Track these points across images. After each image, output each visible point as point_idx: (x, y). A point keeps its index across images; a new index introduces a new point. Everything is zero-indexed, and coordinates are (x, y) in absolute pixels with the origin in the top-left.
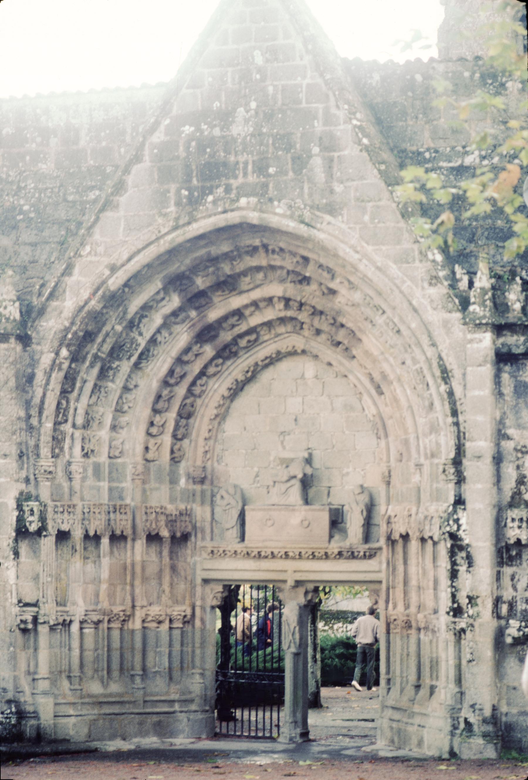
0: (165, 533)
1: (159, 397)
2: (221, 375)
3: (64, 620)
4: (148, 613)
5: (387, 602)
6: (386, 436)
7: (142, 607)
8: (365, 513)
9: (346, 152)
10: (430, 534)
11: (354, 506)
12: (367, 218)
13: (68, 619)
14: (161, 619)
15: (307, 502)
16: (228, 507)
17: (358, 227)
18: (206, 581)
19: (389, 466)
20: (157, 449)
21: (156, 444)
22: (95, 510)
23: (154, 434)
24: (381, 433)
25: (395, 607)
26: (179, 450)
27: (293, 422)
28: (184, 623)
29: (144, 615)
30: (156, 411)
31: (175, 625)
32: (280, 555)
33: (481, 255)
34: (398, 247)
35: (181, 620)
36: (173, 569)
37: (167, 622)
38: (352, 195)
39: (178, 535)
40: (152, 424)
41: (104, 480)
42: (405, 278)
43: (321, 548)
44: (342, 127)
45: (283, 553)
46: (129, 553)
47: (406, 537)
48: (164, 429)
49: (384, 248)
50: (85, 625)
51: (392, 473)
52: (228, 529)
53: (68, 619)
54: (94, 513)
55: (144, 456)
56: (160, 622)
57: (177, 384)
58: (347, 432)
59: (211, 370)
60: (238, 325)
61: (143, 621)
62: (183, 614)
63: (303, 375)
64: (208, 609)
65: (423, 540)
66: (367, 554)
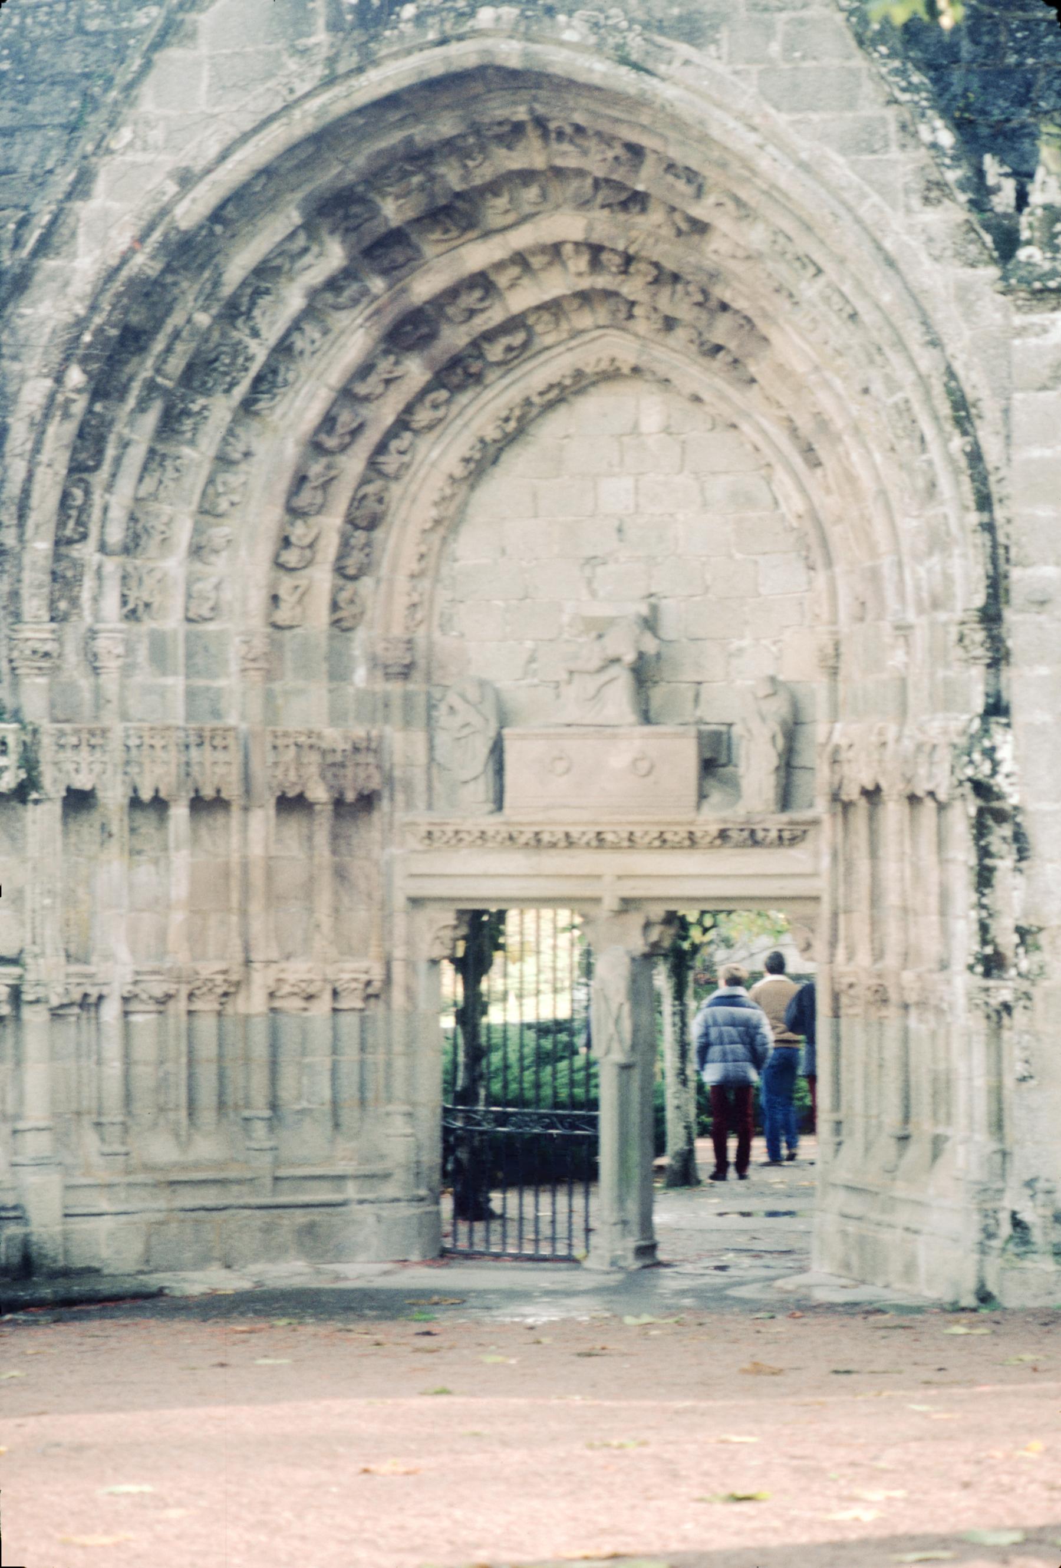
0: (319, 793)
1: (301, 480)
2: (446, 429)
3: (86, 996)
4: (282, 976)
5: (833, 944)
6: (829, 563)
7: (269, 962)
8: (780, 742)
10: (930, 787)
11: (755, 725)
12: (775, 48)
13: (94, 992)
14: (312, 990)
15: (646, 717)
17: (755, 69)
18: (416, 902)
19: (835, 633)
20: (300, 601)
21: (296, 587)
22: (153, 742)
23: (292, 565)
24: (817, 555)
25: (850, 957)
26: (352, 601)
28: (368, 997)
29: (271, 983)
30: (294, 512)
31: (343, 1004)
32: (585, 839)
33: (1044, 129)
34: (849, 115)
36: (340, 874)
37: (327, 996)
39: (350, 796)
40: (286, 542)
42: (867, 189)
43: (678, 824)
45: (591, 835)
46: (235, 840)
47: (873, 795)
48: (314, 553)
49: (815, 117)
50: (134, 1006)
51: (843, 649)
52: (466, 782)
53: (94, 992)
54: (152, 747)
55: (269, 615)
56: (310, 997)
57: (343, 448)
58: (738, 556)
59: (423, 416)
60: (482, 310)
61: (272, 995)
62: (364, 978)
63: (636, 425)
64: (423, 966)
65: (913, 799)
66: (786, 835)
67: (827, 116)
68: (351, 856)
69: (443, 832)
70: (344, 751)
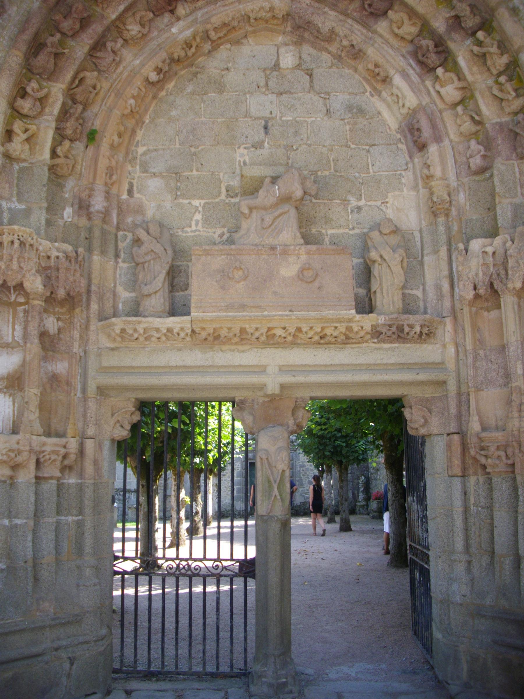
14: (19, 459)
15: (308, 239)
16: (148, 258)
23: (25, 111)
27: (262, 131)
31: (46, 472)
32: (257, 334)
35: (58, 463)
39: (61, 293)
43: (339, 321)
48: (43, 108)
52: (149, 295)
62: (63, 451)
63: (276, 67)
68: (54, 351)
69: (135, 330)
70: (58, 257)
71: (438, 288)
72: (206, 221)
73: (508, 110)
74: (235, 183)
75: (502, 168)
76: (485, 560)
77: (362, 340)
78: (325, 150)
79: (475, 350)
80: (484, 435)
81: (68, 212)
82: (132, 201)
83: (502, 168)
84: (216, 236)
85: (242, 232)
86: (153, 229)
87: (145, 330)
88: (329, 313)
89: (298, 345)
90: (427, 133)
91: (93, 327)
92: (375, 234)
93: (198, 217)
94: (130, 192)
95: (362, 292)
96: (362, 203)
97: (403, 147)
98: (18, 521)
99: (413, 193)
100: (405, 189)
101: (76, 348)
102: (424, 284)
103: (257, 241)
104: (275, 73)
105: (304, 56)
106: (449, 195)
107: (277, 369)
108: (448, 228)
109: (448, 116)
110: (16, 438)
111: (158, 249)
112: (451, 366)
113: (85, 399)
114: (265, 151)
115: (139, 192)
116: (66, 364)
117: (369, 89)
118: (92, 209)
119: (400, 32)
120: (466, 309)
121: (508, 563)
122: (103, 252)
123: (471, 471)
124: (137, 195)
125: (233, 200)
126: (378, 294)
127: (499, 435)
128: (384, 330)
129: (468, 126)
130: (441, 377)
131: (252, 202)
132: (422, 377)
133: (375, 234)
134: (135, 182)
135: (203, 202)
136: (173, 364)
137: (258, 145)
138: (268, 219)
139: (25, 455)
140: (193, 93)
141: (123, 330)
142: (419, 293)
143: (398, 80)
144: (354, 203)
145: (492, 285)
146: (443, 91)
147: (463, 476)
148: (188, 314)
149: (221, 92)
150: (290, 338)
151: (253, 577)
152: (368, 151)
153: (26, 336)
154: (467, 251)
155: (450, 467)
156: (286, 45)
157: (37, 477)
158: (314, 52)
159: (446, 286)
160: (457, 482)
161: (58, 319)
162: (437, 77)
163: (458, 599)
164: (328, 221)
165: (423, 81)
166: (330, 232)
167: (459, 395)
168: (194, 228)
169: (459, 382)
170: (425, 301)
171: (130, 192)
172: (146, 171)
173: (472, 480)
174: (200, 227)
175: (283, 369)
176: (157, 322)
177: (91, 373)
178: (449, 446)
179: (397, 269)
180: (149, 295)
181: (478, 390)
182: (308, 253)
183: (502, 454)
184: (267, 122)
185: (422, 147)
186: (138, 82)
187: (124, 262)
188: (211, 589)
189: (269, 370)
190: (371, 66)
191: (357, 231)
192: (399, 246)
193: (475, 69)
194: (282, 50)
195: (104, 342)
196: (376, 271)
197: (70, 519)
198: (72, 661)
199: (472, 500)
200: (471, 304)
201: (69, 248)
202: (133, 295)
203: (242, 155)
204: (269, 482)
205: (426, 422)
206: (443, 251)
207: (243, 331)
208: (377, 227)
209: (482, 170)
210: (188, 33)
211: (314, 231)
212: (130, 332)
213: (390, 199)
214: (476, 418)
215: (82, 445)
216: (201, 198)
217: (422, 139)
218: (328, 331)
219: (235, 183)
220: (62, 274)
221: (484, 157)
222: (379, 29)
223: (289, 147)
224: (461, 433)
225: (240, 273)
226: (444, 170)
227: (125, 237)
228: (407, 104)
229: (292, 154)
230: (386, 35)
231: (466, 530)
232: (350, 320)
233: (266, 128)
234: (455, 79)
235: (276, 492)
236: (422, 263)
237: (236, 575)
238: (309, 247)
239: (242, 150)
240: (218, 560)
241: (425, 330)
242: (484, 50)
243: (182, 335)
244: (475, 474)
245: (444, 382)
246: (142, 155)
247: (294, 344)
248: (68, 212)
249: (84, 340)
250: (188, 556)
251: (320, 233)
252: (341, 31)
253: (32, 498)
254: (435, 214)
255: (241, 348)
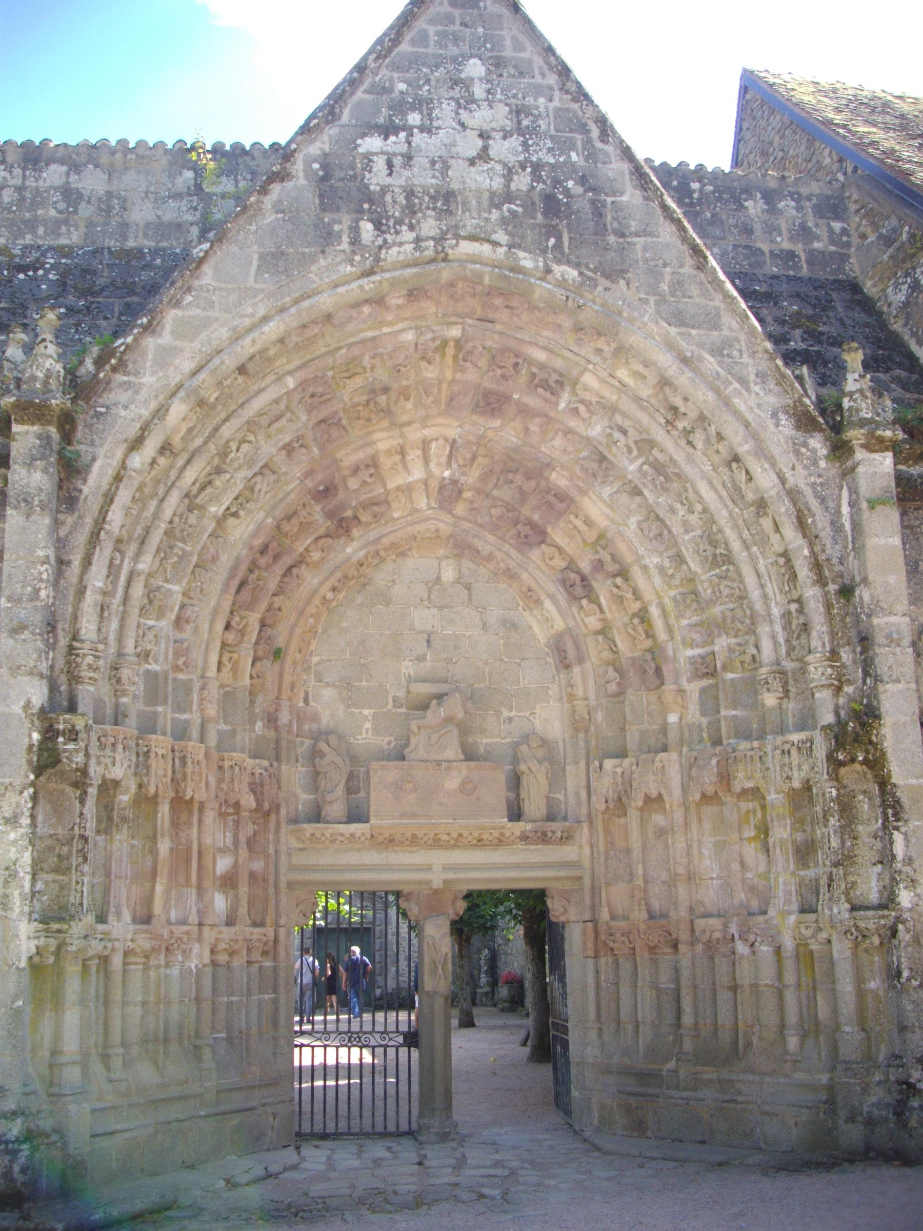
4: (221, 936)
7: (212, 926)
9: (624, 198)
12: (664, 287)
14: (236, 947)
17: (652, 299)
18: (291, 885)
19: (588, 706)
23: (229, 642)
27: (425, 645)
29: (212, 941)
32: (425, 839)
34: (715, 333)
37: (245, 952)
38: (639, 255)
40: (228, 627)
41: (165, 703)
42: (730, 378)
43: (494, 828)
44: (614, 166)
45: (431, 836)
48: (243, 636)
49: (693, 332)
50: (132, 959)
52: (331, 802)
57: (268, 567)
61: (212, 952)
62: (265, 939)
63: (438, 579)
67: (702, 332)
69: (323, 835)
71: (577, 795)
72: (376, 730)
73: (639, 647)
74: (401, 694)
75: (633, 698)
76: (613, 1027)
77: (513, 843)
78: (481, 664)
79: (607, 852)
80: (612, 923)
81: (259, 725)
82: (308, 708)
83: (633, 698)
84: (384, 744)
85: (411, 747)
86: (332, 739)
87: (332, 835)
88: (485, 821)
89: (458, 847)
90: (571, 654)
91: (283, 830)
92: (524, 748)
93: (368, 725)
94: (306, 700)
95: (512, 795)
96: (514, 713)
97: (550, 660)
98: (234, 999)
99: (558, 705)
100: (551, 702)
101: (271, 850)
102: (565, 789)
103: (425, 757)
104: (437, 587)
105: (465, 571)
106: (589, 714)
107: (440, 867)
108: (587, 742)
109: (590, 640)
110: (233, 929)
111: (338, 760)
112: (587, 864)
113: (277, 893)
114: (428, 665)
115: (314, 701)
116: (262, 864)
117: (521, 603)
118: (279, 723)
119: (552, 563)
120: (600, 817)
121: (630, 1028)
122: (288, 761)
123: (602, 953)
124: (312, 703)
125: (399, 710)
126: (526, 801)
127: (622, 924)
128: (531, 835)
129: (606, 655)
130: (578, 873)
131: (421, 722)
132: (562, 873)
133: (524, 748)
134: (310, 690)
135: (372, 711)
136: (353, 862)
137: (421, 659)
138: (435, 737)
139: (241, 942)
140: (362, 605)
141: (313, 835)
142: (561, 797)
143: (548, 604)
144: (506, 713)
145: (620, 799)
146: (587, 620)
147: (596, 957)
148: (367, 821)
149: (388, 605)
150: (452, 842)
151: (416, 1046)
152: (519, 665)
153: (236, 842)
154: (601, 768)
155: (585, 950)
156: (448, 558)
157: (248, 962)
158: (473, 566)
159: (584, 795)
160: (590, 963)
161: (254, 823)
162: (582, 607)
163: (591, 1060)
164: (483, 731)
165: (570, 607)
166: (485, 741)
167: (593, 888)
168: (364, 736)
169: (593, 878)
170: (566, 804)
171: (306, 700)
172: (320, 681)
173: (603, 960)
174: (370, 735)
175: (446, 868)
176: (342, 827)
177: (283, 870)
178: (584, 931)
179: (543, 780)
180: (331, 802)
181: (608, 884)
182: (469, 768)
183: (626, 939)
184: (429, 635)
185: (568, 667)
186: (317, 601)
187: (302, 766)
188: (331, 1083)
189: (434, 868)
190: (525, 589)
191: (508, 740)
192: (545, 759)
193: (614, 607)
194: (444, 563)
195: (296, 844)
196: (524, 782)
197: (266, 996)
198: (275, 1115)
199: (603, 978)
200: (604, 813)
201: (265, 763)
202: (312, 797)
203: (407, 668)
204: (435, 963)
205: (565, 910)
206: (583, 763)
207: (414, 836)
208: (526, 738)
209: (618, 694)
210: (362, 554)
211: (470, 740)
212: (319, 836)
213: (538, 711)
214: (606, 909)
215: (276, 932)
216: (370, 708)
217: (567, 661)
218: (485, 836)
219: (401, 694)
220: (266, 789)
221: (619, 684)
222: (533, 557)
223: (449, 661)
224: (594, 921)
225: (411, 786)
226: (585, 691)
227: (302, 743)
228: (556, 627)
229: (451, 667)
230: (539, 563)
231: (598, 1002)
232: (503, 828)
233: (428, 641)
234: (597, 611)
235: (440, 972)
236: (564, 770)
237: (402, 1045)
238: (469, 763)
239: (406, 663)
240: (385, 1032)
241: (565, 835)
242: (621, 593)
243: (363, 839)
244: (606, 955)
245: (581, 878)
246: (316, 665)
247: (455, 846)
248: (259, 725)
249: (277, 842)
250: (358, 1029)
251: (476, 742)
252: (499, 555)
253: (245, 980)
254: (577, 730)
255: (410, 849)
